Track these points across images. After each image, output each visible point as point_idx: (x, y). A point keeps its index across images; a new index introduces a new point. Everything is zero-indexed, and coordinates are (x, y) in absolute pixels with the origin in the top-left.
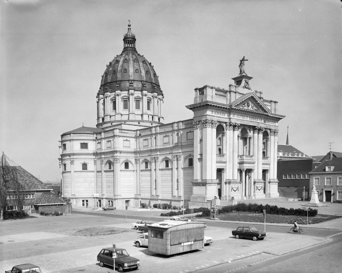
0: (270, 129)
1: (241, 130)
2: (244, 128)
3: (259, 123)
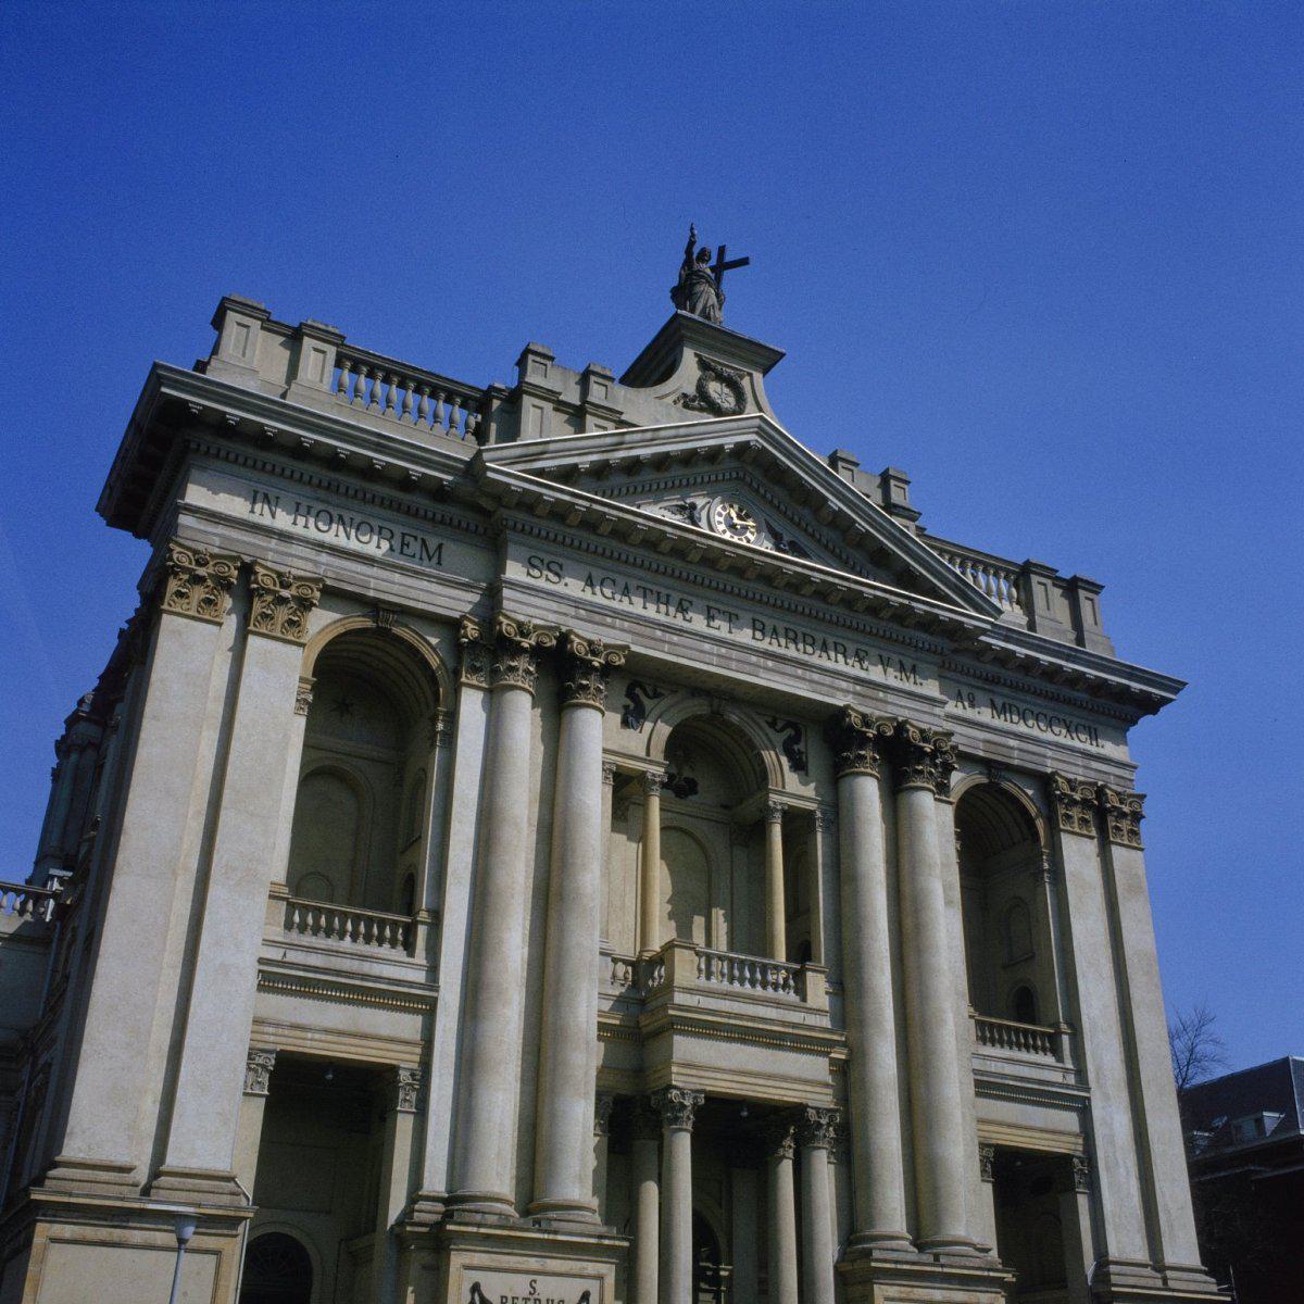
0: (1045, 781)
1: (664, 730)
2: (715, 717)
3: (886, 688)
